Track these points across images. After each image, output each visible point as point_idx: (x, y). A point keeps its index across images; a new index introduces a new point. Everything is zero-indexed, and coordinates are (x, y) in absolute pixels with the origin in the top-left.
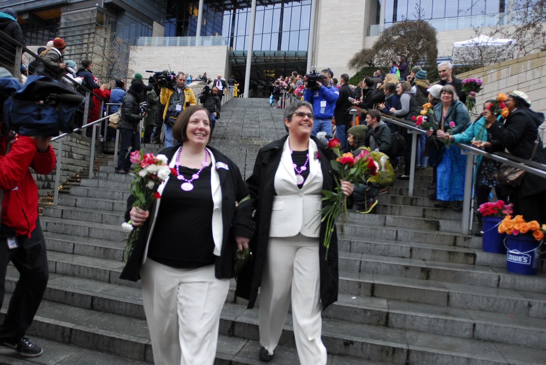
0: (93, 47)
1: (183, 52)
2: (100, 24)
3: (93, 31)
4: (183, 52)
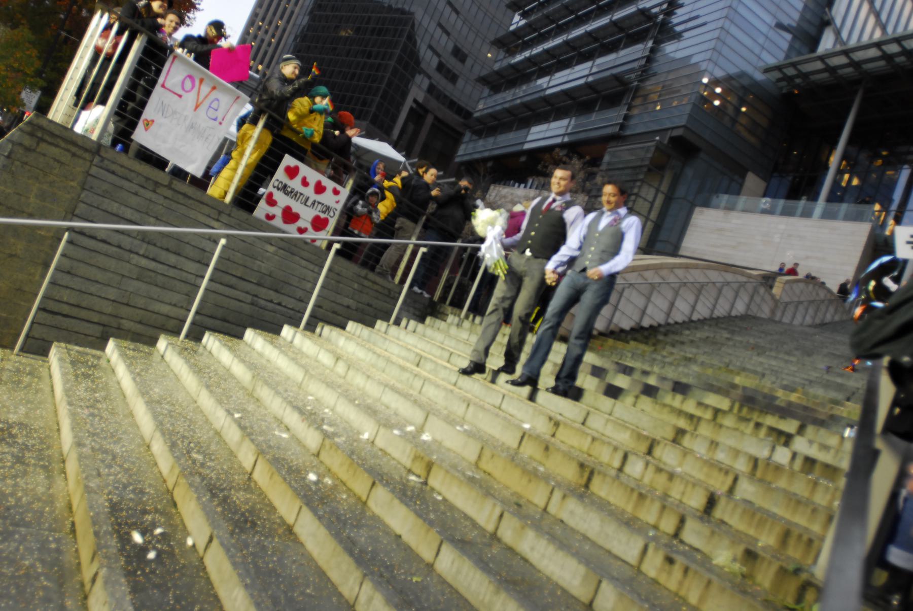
0: (634, 201)
1: (782, 227)
2: (656, 168)
3: (641, 177)
4: (782, 227)
